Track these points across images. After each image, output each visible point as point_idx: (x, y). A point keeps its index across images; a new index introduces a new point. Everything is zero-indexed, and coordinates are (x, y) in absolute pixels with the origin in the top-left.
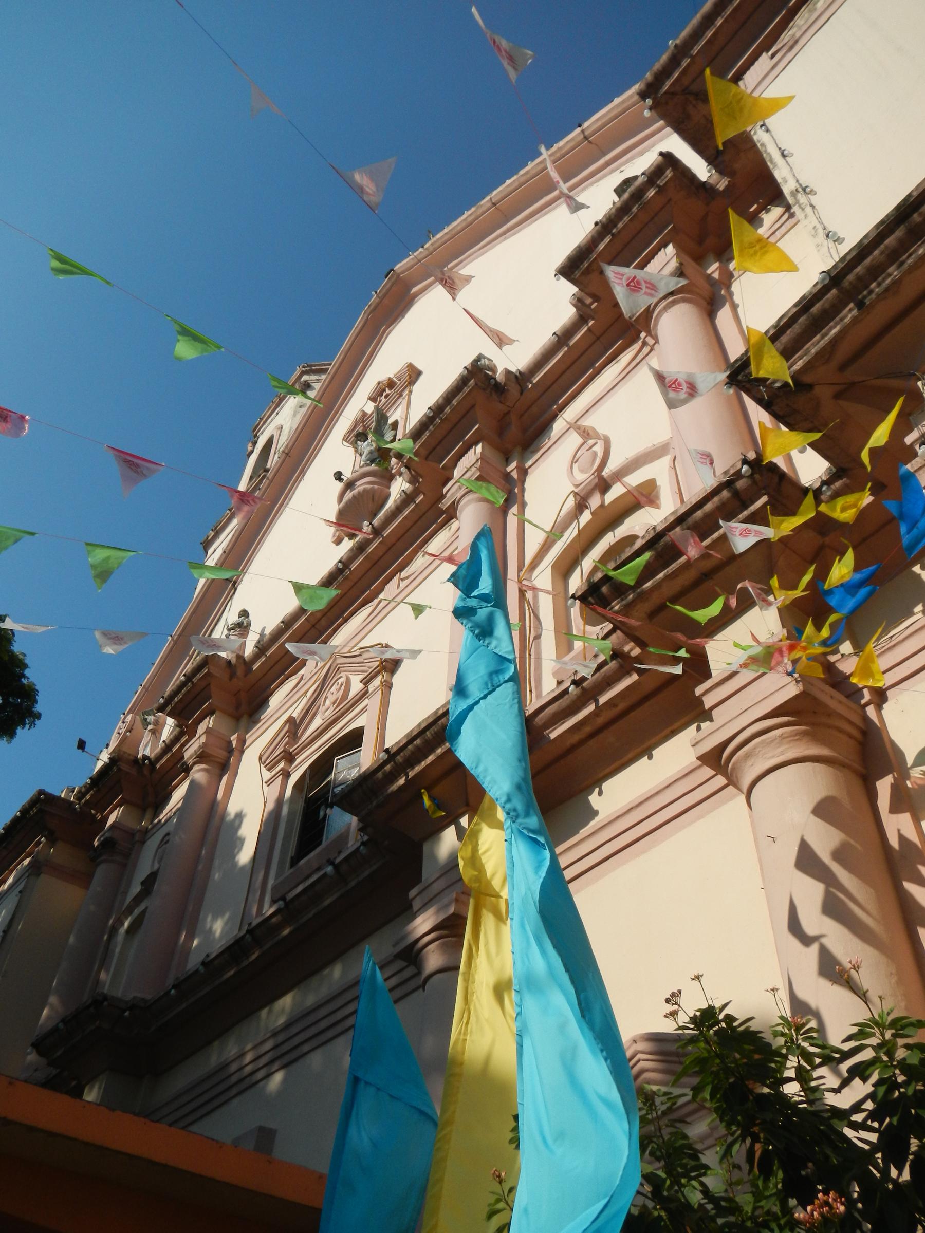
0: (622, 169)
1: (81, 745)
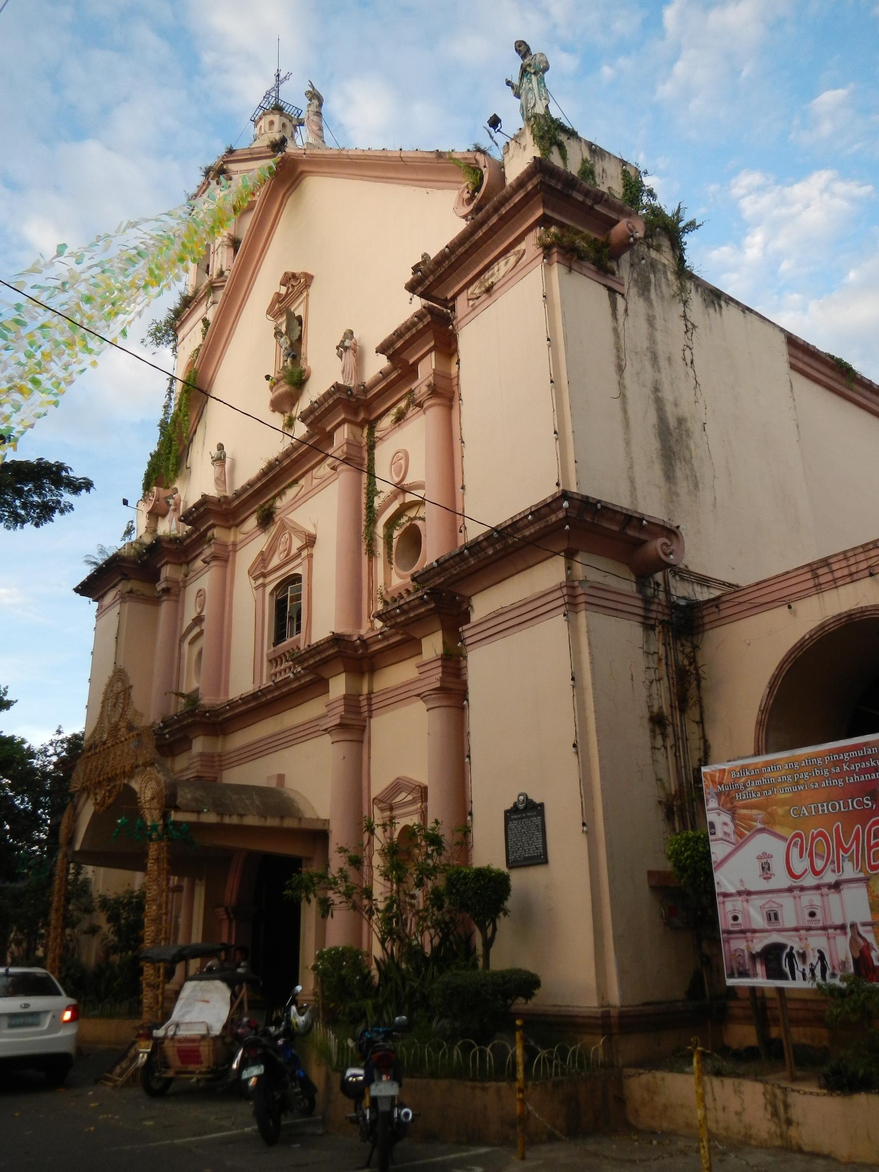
0: (429, 190)
1: (125, 502)
